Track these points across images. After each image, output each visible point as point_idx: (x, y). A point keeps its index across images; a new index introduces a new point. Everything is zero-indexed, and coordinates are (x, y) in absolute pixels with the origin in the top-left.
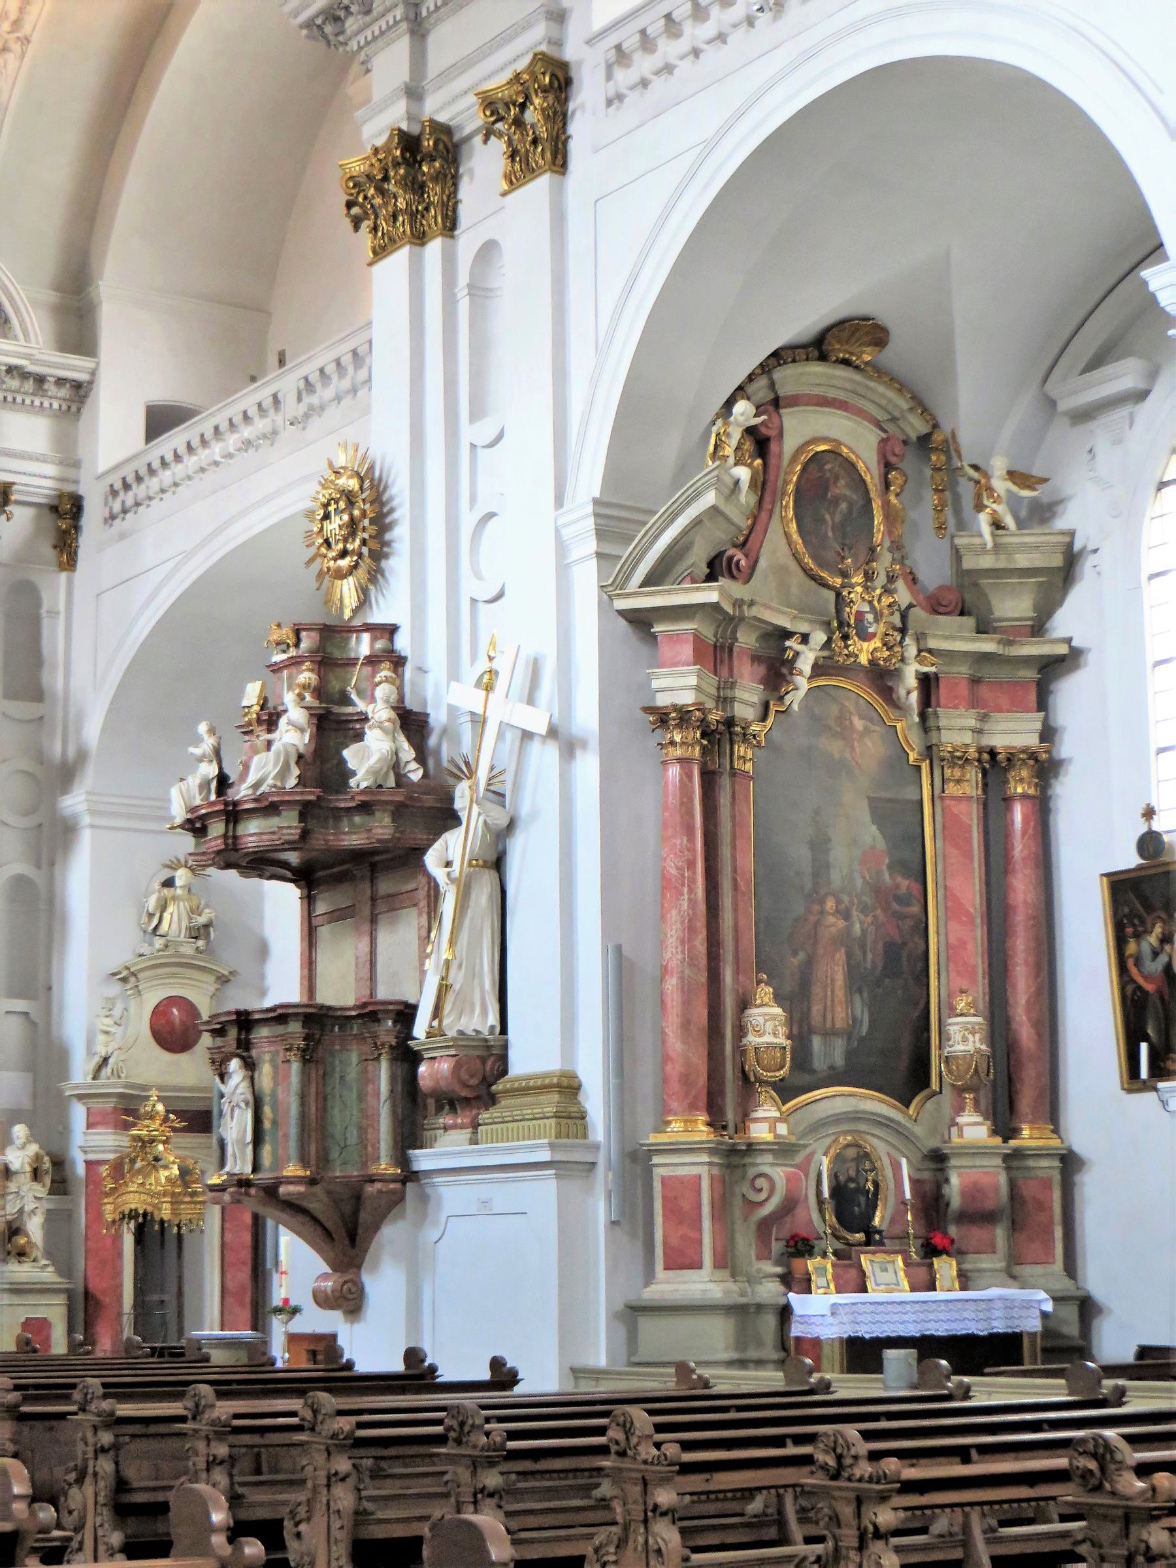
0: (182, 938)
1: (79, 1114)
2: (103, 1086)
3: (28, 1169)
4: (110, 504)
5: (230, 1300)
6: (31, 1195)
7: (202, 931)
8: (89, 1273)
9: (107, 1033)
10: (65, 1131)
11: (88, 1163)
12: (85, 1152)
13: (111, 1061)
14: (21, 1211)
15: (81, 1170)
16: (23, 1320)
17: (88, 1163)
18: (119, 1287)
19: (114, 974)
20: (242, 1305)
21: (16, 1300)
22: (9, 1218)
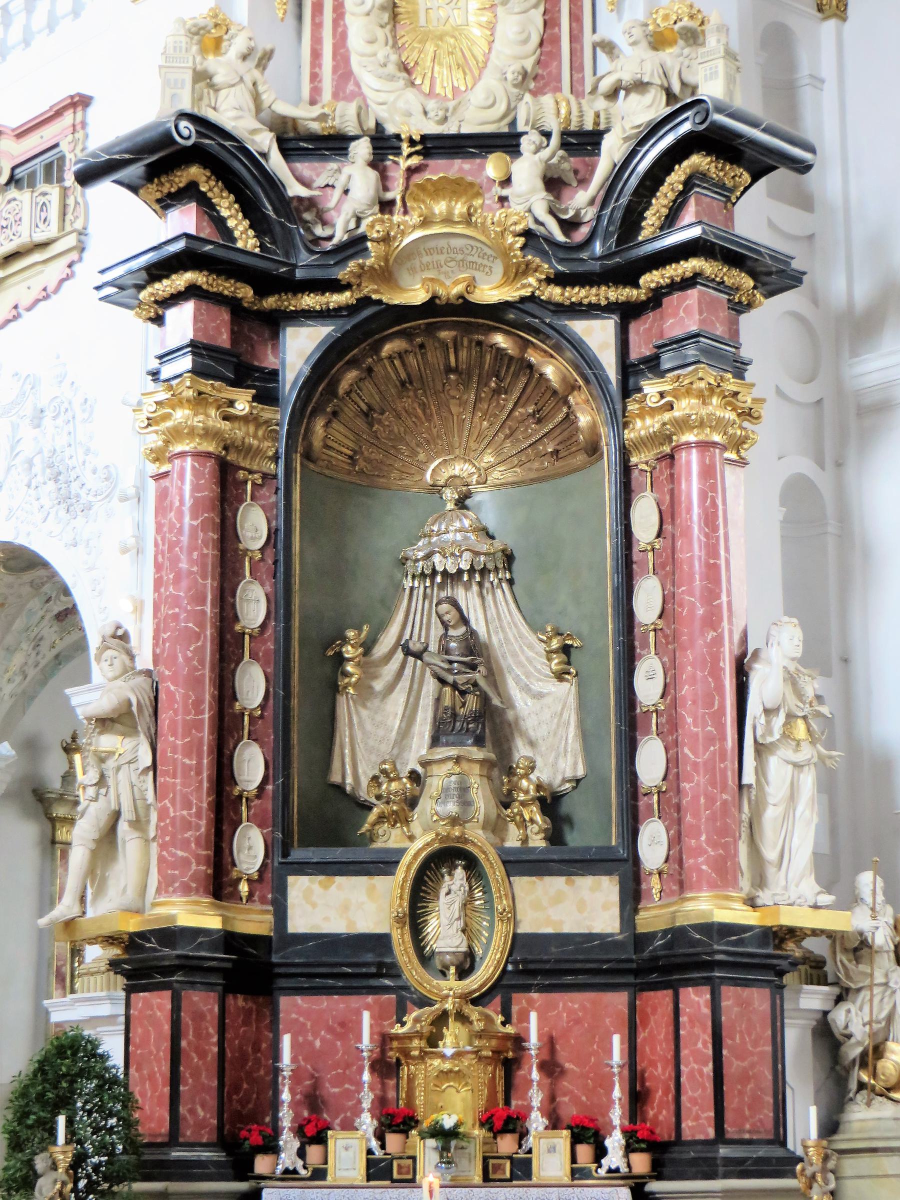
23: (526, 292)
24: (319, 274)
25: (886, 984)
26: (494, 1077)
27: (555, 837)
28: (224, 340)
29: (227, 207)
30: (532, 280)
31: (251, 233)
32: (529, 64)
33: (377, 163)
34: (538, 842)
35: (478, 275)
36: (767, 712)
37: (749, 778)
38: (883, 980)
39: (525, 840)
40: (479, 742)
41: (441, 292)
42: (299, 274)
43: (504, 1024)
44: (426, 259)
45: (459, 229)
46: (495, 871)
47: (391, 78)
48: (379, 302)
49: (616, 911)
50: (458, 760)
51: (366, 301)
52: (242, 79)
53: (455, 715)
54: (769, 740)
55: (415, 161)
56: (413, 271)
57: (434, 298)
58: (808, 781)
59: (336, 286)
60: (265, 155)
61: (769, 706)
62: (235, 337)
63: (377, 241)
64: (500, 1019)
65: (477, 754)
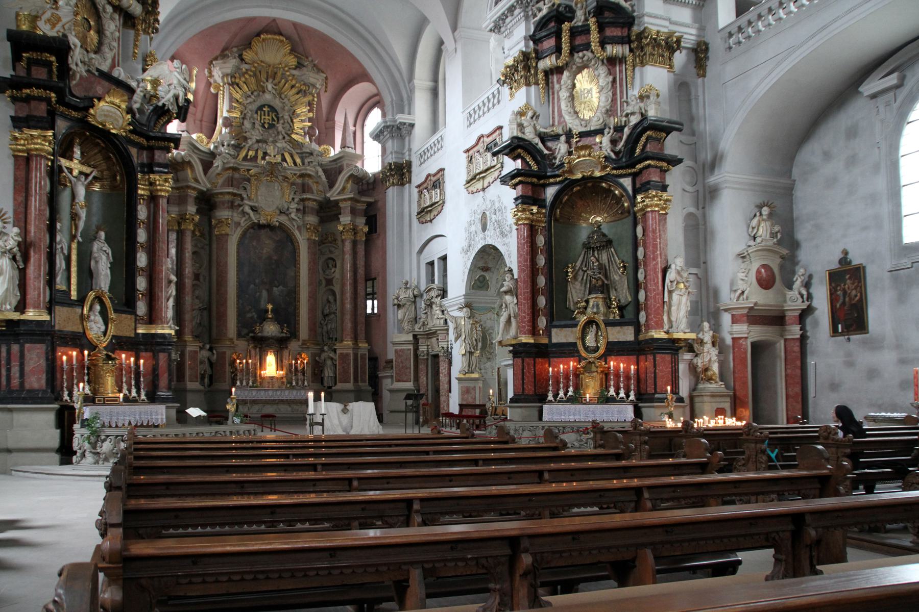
8: (737, 387)
9: (743, 280)
11: (733, 339)
13: (746, 293)
14: (710, 360)
17: (733, 339)
24: (553, 173)
27: (622, 316)
28: (530, 194)
29: (528, 159)
32: (608, 107)
33: (568, 142)
34: (617, 318)
36: (671, 282)
37: (666, 299)
39: (614, 317)
40: (602, 292)
42: (549, 174)
45: (588, 158)
46: (602, 326)
47: (572, 116)
50: (596, 298)
51: (566, 179)
53: (595, 286)
55: (578, 139)
58: (684, 299)
59: (558, 176)
60: (537, 144)
62: (533, 192)
65: (601, 296)
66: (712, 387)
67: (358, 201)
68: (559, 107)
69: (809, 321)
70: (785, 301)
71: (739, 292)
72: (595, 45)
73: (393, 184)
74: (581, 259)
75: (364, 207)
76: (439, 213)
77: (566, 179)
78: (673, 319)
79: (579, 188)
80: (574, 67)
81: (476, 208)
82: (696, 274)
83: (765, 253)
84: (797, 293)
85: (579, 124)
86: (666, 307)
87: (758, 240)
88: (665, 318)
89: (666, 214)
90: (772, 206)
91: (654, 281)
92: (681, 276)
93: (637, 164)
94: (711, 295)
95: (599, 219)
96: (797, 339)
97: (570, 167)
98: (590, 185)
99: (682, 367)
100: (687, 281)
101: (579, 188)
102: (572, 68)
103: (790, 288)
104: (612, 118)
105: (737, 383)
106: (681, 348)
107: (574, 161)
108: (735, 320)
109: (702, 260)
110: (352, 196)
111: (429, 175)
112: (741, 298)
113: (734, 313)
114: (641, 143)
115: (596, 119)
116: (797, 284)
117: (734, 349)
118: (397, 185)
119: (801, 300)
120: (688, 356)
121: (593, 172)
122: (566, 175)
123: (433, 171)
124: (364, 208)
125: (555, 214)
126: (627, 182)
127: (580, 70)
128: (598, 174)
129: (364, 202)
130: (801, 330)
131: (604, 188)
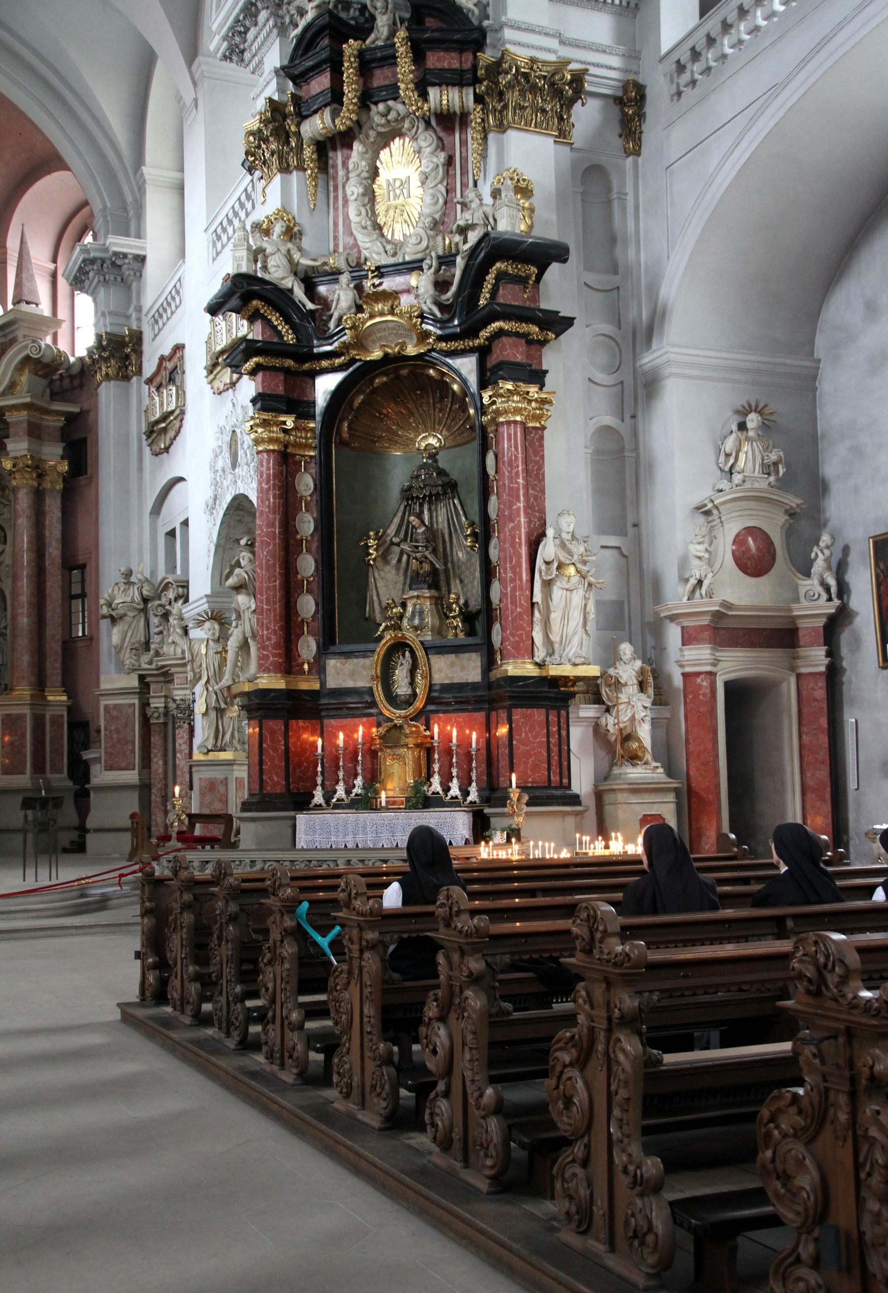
0: (756, 474)
1: (673, 634)
2: (696, 606)
3: (635, 682)
4: (675, 80)
5: (810, 796)
6: (639, 704)
7: (772, 468)
9: (700, 558)
10: (661, 648)
12: (682, 666)
13: (706, 583)
14: (633, 718)
15: (678, 681)
16: (640, 817)
18: (718, 786)
19: (698, 508)
20: (823, 800)
21: (634, 799)
22: (622, 725)
23: (430, 347)
25: (629, 703)
26: (419, 756)
30: (431, 340)
31: (290, 332)
35: (407, 340)
38: (627, 700)
41: (389, 351)
43: (425, 730)
44: (378, 335)
45: (389, 318)
48: (360, 360)
49: (479, 671)
52: (279, 250)
54: (549, 578)
56: (374, 342)
57: (386, 355)
58: (577, 598)
61: (547, 560)
63: (350, 329)
64: (423, 728)
66: (635, 773)
67: (47, 412)
68: (346, 217)
69: (845, 638)
70: (797, 600)
71: (693, 581)
72: (406, 89)
73: (107, 377)
74: (397, 520)
75: (60, 422)
76: (178, 432)
77: (353, 361)
78: (555, 637)
79: (385, 379)
80: (372, 134)
81: (223, 422)
82: (618, 548)
83: (752, 504)
84: (815, 581)
85: (381, 250)
86: (537, 614)
87: (737, 478)
88: (538, 635)
89: (543, 428)
90: (753, 407)
91: (511, 562)
92: (571, 554)
93: (481, 329)
94: (648, 589)
95: (433, 441)
96: (819, 674)
97: (357, 337)
98: (404, 372)
99: (578, 734)
100: (585, 563)
101: (385, 379)
102: (367, 137)
103: (808, 574)
104: (439, 238)
105: (692, 764)
106: (573, 695)
107: (364, 323)
108: (688, 639)
109: (630, 519)
110: (28, 400)
111: (162, 359)
112: (697, 593)
113: (686, 624)
114: (487, 287)
115: (413, 240)
116: (819, 565)
117: (685, 697)
118: (116, 378)
119: (824, 596)
120: (588, 711)
121: (403, 346)
122: (353, 352)
123: (167, 352)
124: (61, 424)
125: (339, 432)
126: (467, 366)
127: (385, 140)
128: (411, 350)
129: (59, 413)
130: (827, 656)
131: (430, 377)
